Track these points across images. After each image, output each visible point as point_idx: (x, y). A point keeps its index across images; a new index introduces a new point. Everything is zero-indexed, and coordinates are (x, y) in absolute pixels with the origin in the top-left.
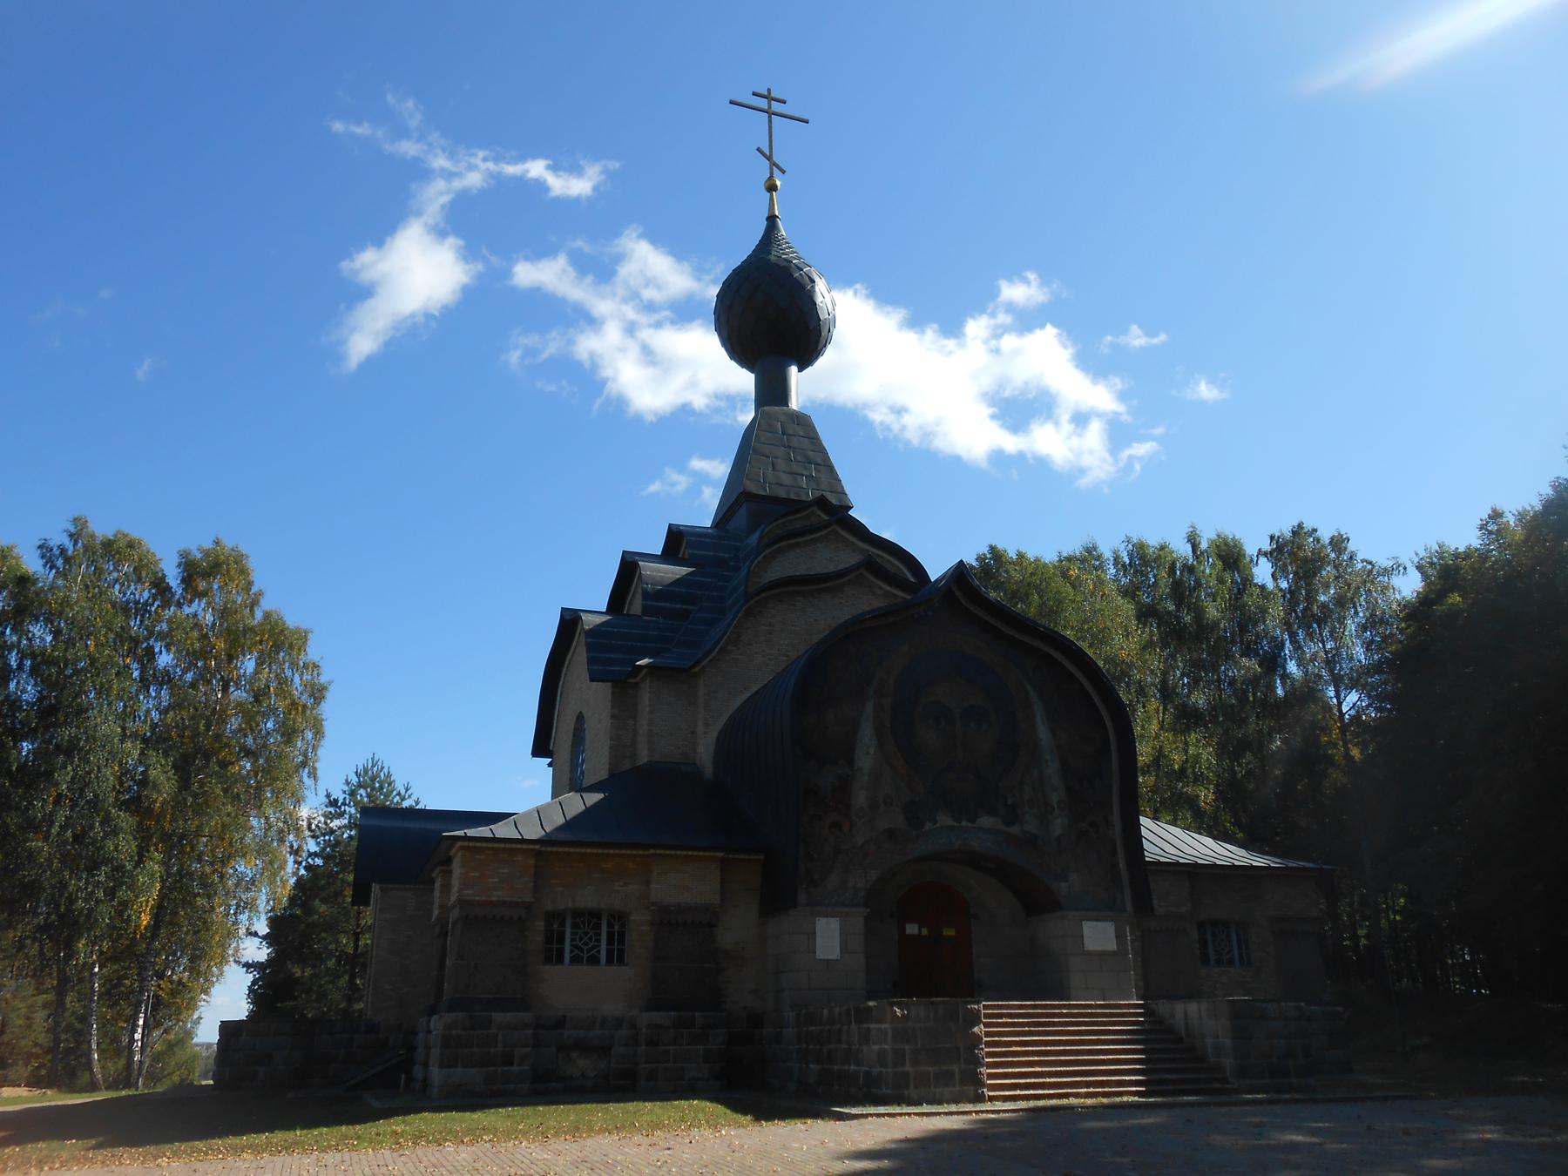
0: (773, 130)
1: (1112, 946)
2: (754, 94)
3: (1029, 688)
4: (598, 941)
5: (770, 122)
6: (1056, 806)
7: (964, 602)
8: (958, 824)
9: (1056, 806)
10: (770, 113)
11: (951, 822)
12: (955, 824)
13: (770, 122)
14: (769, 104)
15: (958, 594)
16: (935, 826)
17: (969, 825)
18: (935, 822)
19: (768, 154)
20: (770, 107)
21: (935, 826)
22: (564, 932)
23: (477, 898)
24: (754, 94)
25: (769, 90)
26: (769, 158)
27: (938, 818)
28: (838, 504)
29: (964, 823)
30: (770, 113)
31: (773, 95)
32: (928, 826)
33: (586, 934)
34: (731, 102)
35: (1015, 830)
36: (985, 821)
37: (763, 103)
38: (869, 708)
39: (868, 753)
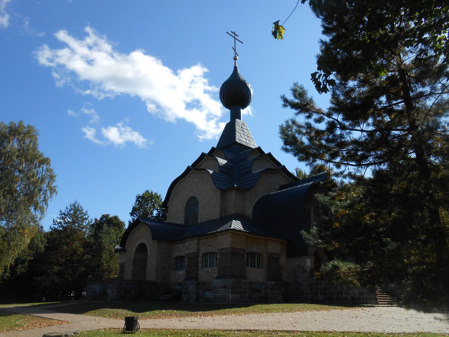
0: (234, 43)
2: (232, 32)
4: (255, 261)
5: (235, 41)
10: (235, 39)
13: (235, 41)
14: (234, 35)
19: (234, 49)
20: (235, 37)
22: (208, 259)
23: (235, 247)
24: (232, 32)
25: (235, 32)
26: (235, 50)
30: (235, 39)
31: (236, 33)
33: (253, 259)
34: (227, 33)
37: (233, 35)
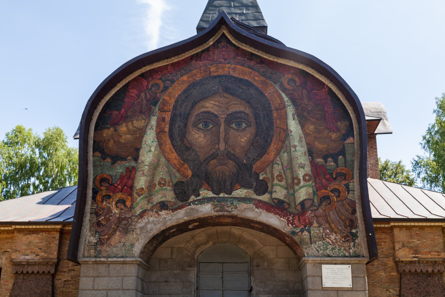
1: (347, 283)
3: (284, 95)
6: (301, 178)
7: (234, 42)
8: (217, 196)
9: (301, 178)
11: (210, 194)
12: (215, 196)
15: (229, 37)
16: (198, 198)
17: (226, 196)
18: (199, 195)
21: (198, 198)
27: (201, 192)
28: (258, 25)
29: (221, 195)
32: (193, 198)
35: (265, 198)
36: (240, 192)
38: (154, 121)
39: (150, 151)
